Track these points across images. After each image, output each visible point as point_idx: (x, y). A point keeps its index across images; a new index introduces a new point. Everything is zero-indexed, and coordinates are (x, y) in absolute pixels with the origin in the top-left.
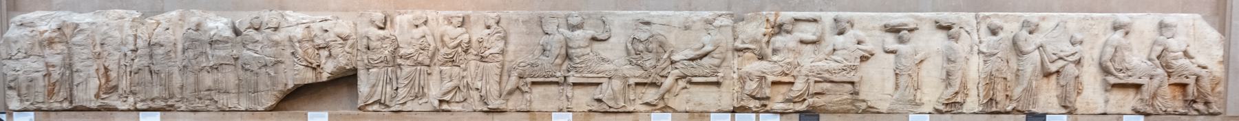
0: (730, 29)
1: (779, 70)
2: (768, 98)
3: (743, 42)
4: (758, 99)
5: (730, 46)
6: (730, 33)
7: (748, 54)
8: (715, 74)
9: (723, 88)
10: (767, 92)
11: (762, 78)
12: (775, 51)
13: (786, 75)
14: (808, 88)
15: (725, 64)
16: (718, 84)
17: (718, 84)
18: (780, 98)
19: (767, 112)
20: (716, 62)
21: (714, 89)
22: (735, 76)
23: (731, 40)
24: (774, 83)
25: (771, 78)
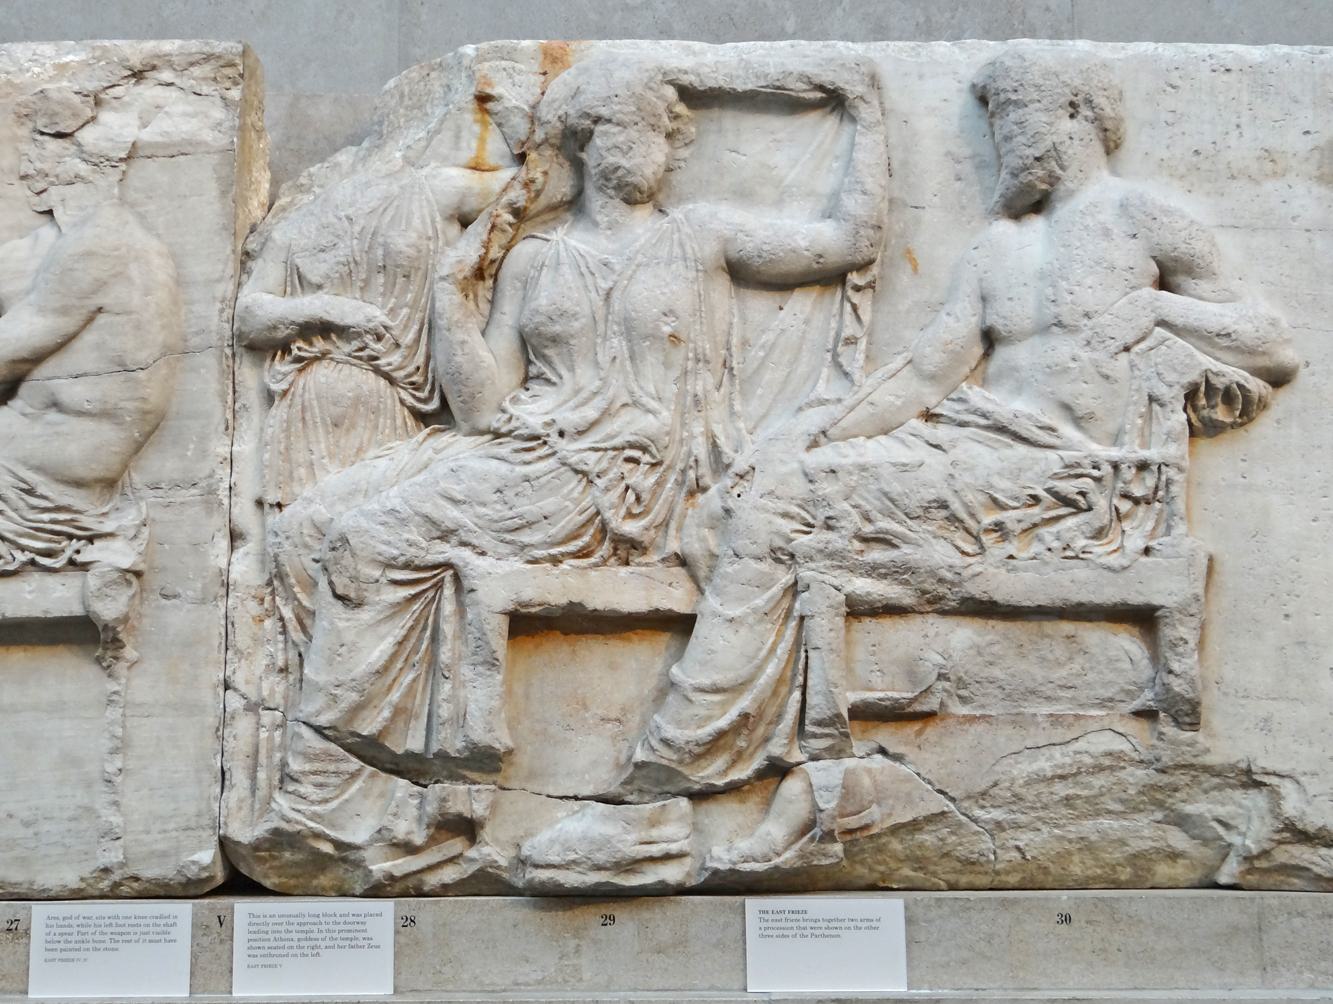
0: (202, 178)
1: (563, 504)
2: (485, 761)
3: (298, 281)
4: (414, 769)
5: (213, 321)
6: (208, 207)
7: (335, 378)
8: (62, 545)
9: (143, 679)
10: (477, 703)
11: (434, 581)
12: (535, 351)
13: (627, 549)
14: (798, 670)
15: (161, 463)
16: (82, 634)
17: (82, 634)
18: (592, 759)
19: (486, 883)
20: (85, 444)
21: (65, 675)
22: (245, 568)
23: (212, 261)
24: (529, 625)
25: (502, 581)
